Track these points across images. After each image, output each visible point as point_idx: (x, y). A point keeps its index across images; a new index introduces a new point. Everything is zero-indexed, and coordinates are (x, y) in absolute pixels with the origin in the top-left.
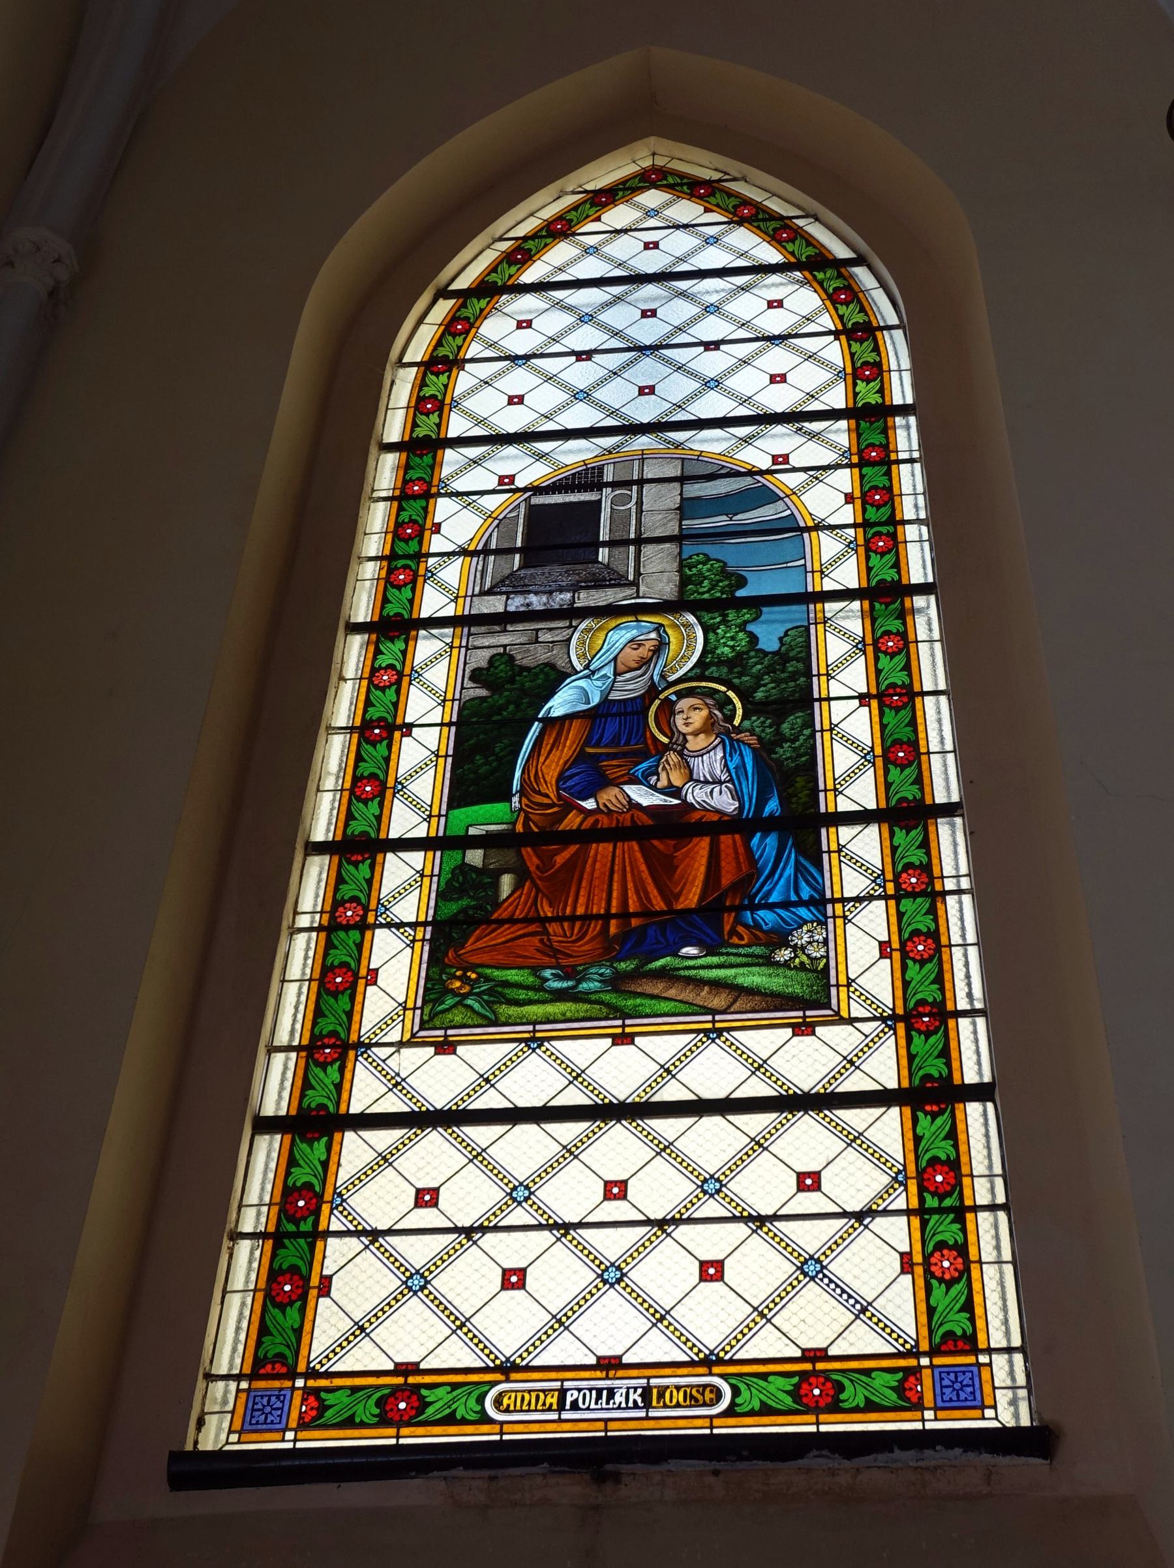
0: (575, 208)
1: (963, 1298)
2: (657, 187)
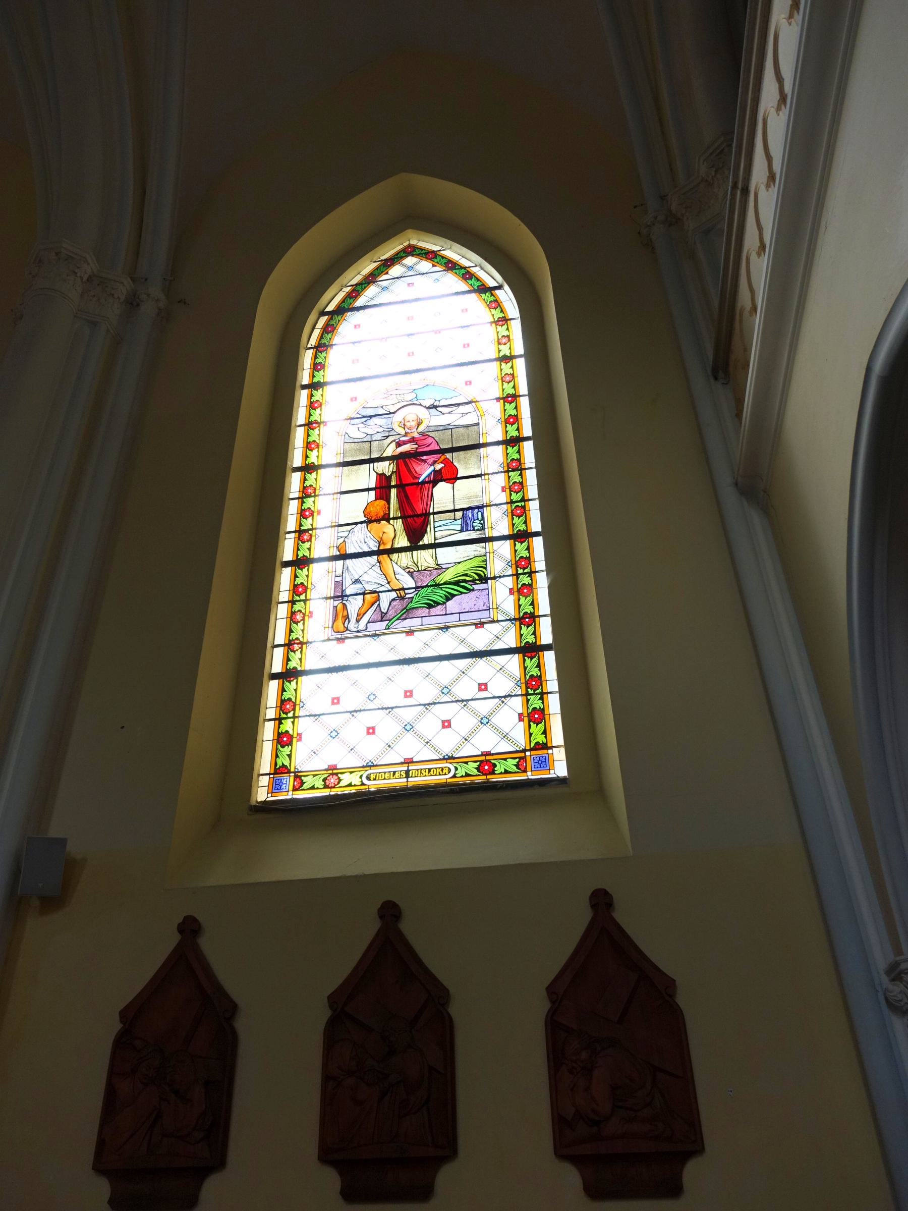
0: (377, 268)
1: (543, 729)
2: (412, 255)
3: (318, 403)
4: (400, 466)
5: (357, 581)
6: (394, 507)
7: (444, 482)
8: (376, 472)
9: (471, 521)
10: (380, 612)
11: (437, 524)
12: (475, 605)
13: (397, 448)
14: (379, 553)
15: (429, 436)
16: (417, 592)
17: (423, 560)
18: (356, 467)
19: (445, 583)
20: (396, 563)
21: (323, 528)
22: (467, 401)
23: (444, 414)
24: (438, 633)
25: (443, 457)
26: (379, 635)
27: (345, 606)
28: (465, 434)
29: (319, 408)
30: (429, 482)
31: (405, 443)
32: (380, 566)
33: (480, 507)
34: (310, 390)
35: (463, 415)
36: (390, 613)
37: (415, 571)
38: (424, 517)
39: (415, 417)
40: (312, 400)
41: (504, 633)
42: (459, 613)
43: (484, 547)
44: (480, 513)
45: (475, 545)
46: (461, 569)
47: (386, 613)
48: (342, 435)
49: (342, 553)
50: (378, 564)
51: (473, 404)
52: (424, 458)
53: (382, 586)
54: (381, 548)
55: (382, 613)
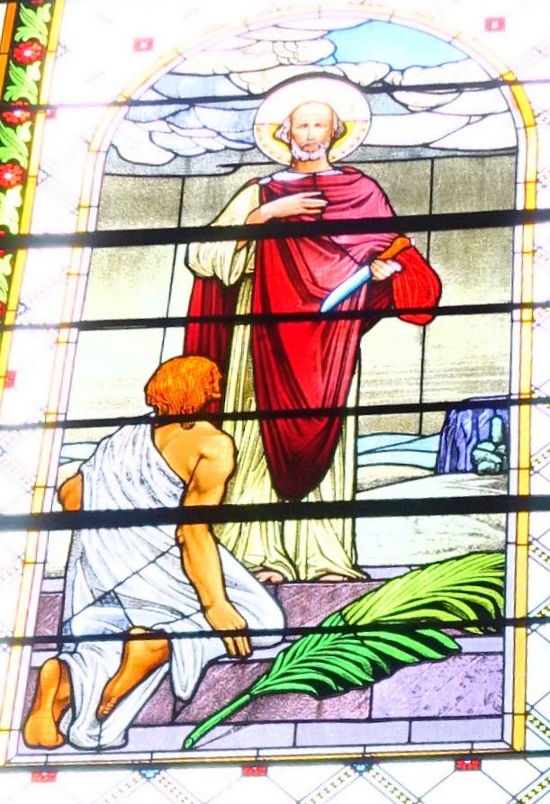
3: (35, 46)
4: (267, 259)
5: (106, 598)
6: (238, 381)
7: (395, 320)
8: (193, 272)
9: (468, 444)
10: (170, 698)
11: (364, 444)
12: (459, 698)
13: (262, 203)
14: (182, 516)
15: (364, 176)
16: (289, 644)
17: (313, 549)
18: (134, 251)
19: (375, 626)
20: (232, 553)
21: (18, 428)
22: (486, 79)
23: (413, 112)
24: (341, 774)
25: (399, 243)
26: (162, 766)
27: (65, 668)
28: (474, 179)
29: (37, 64)
30: (351, 315)
31: (287, 190)
32: (182, 558)
33: (500, 405)
34: (14, 5)
35: (472, 119)
36: (200, 701)
37: (285, 580)
38: (326, 420)
39: (324, 115)
40: (17, 38)
41: (542, 792)
42: (411, 720)
43: (503, 524)
44: (497, 423)
45: (474, 516)
46: (426, 586)
47: (189, 701)
48: (99, 151)
49: (69, 508)
50: (176, 551)
51: (505, 89)
52: (343, 240)
53: (184, 617)
54: (190, 502)
55: (177, 699)
